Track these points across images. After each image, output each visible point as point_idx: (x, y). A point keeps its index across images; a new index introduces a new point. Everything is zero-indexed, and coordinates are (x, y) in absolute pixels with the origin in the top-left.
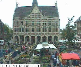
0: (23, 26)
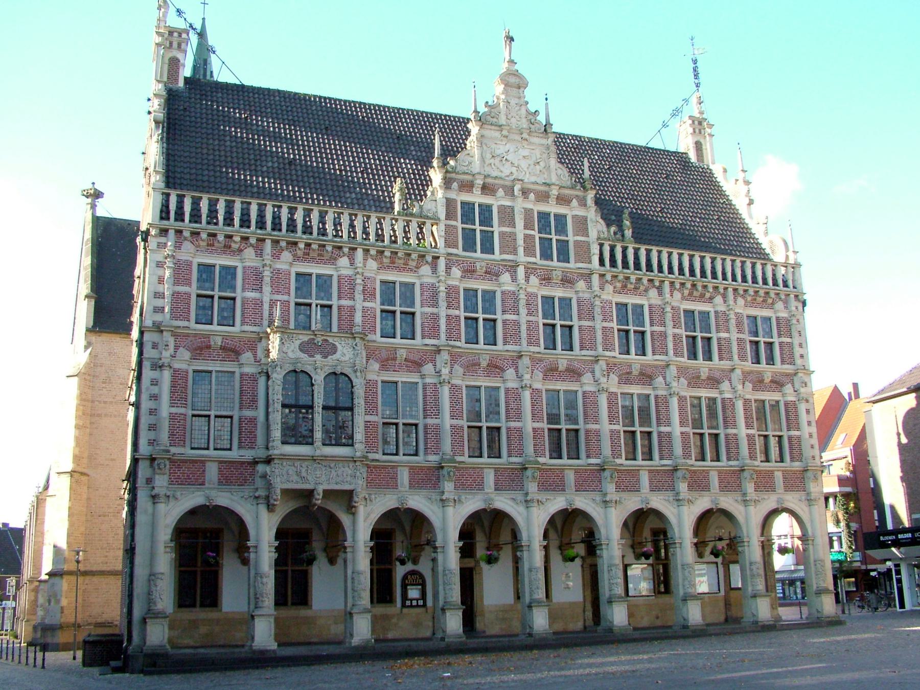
0: (345, 354)
